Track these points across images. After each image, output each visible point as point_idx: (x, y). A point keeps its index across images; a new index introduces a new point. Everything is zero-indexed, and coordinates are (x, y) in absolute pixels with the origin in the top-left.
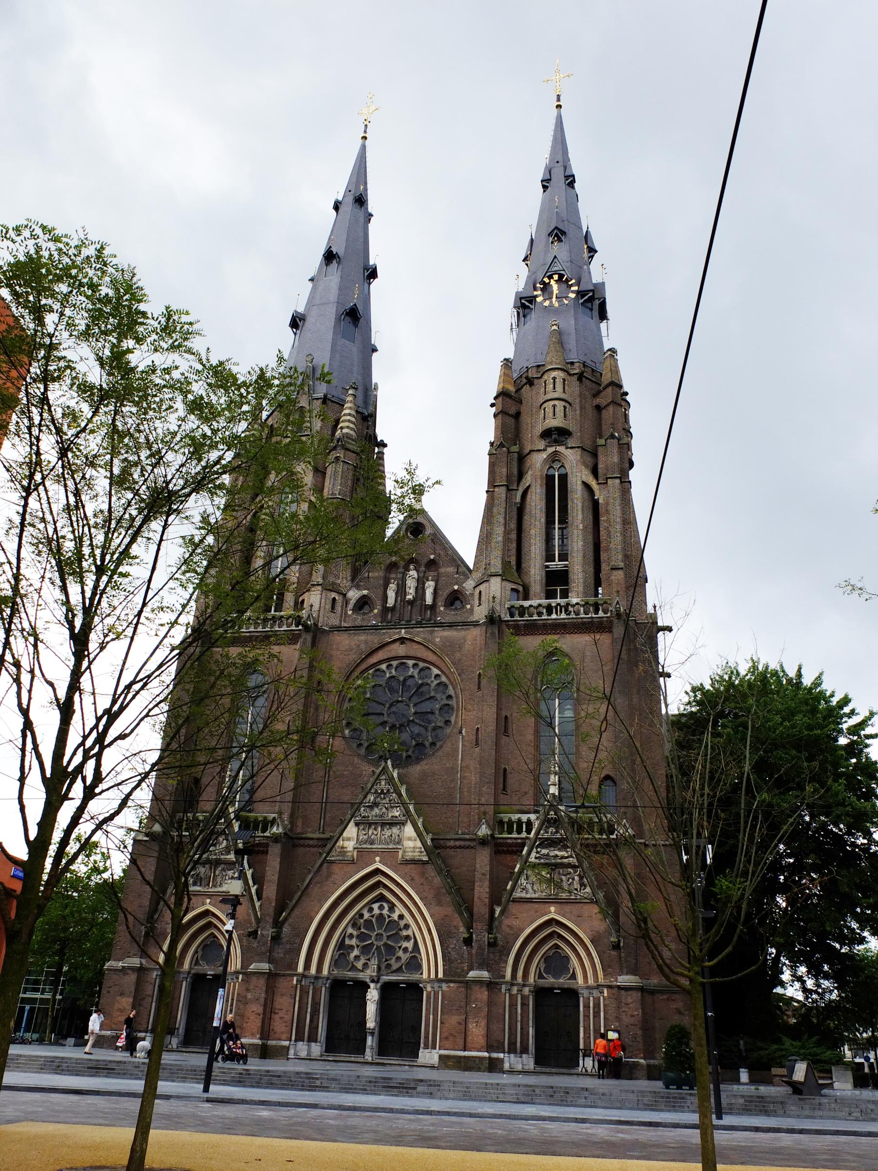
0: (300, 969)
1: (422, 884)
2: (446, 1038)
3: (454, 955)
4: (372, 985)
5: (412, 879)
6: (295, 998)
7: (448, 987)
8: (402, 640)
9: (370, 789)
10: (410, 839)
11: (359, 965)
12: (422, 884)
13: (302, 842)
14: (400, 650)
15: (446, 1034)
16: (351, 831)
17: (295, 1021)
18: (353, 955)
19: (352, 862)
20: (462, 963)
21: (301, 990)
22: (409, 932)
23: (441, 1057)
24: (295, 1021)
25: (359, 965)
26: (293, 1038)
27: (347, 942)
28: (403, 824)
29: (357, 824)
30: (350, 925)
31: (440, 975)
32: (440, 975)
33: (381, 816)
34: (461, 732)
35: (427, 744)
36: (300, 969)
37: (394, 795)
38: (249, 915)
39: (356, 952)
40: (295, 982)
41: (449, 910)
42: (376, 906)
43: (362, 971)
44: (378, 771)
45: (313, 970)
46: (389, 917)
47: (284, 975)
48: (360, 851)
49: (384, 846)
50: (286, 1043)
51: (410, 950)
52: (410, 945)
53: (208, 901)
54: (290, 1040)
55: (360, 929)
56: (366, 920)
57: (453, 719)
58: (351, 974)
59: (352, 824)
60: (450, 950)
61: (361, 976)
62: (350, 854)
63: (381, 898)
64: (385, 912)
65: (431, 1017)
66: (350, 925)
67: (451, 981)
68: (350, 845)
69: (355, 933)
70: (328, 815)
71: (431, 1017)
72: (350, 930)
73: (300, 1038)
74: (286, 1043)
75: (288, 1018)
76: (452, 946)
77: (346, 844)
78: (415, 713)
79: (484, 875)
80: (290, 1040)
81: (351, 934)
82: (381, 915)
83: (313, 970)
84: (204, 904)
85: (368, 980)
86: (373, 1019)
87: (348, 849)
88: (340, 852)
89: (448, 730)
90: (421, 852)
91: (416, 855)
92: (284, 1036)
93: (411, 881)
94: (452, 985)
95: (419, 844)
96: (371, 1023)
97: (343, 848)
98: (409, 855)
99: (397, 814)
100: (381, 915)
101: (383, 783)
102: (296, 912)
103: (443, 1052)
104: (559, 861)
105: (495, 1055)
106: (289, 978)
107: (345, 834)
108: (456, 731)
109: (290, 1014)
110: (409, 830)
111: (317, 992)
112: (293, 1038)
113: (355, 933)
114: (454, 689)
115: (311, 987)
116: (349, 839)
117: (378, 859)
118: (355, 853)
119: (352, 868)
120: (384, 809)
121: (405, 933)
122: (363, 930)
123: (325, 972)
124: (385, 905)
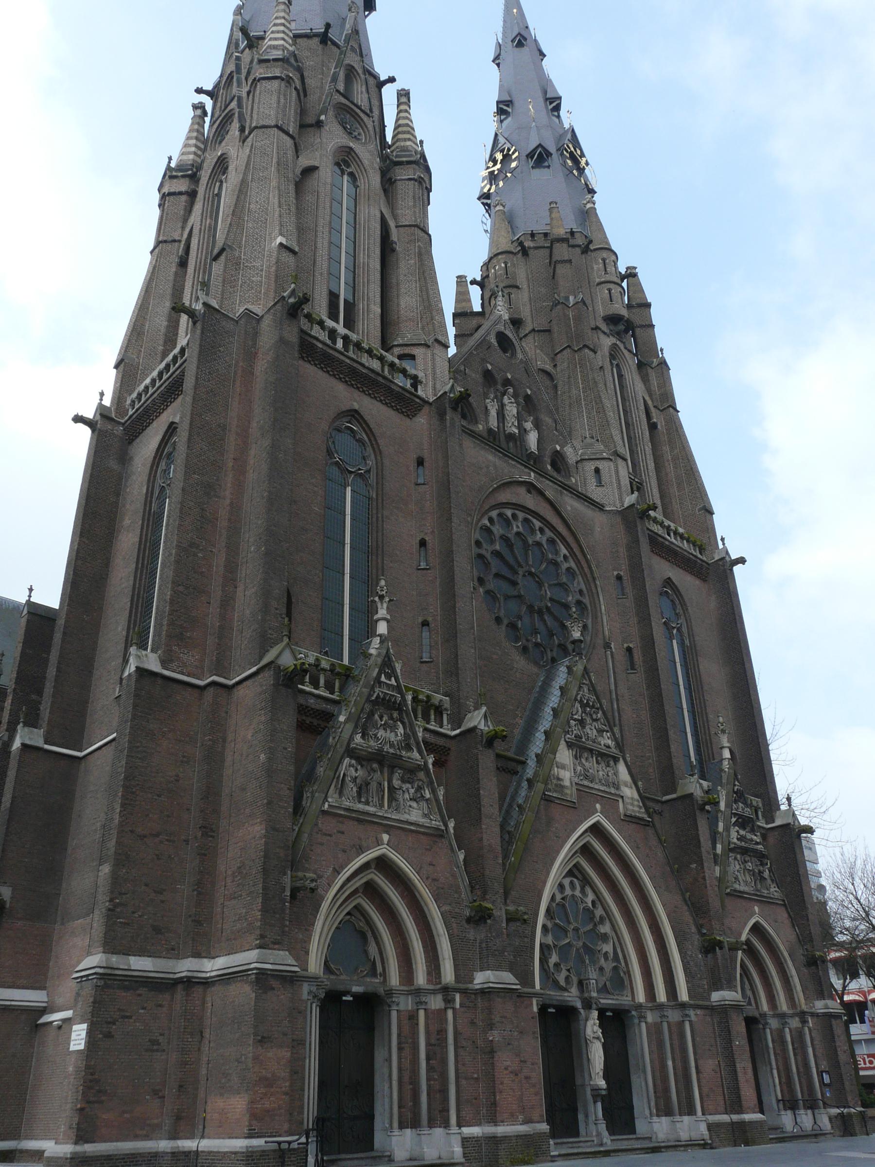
5: (638, 847)
8: (530, 487)
14: (530, 501)
22: (605, 928)
23: (710, 1127)
28: (616, 760)
31: (684, 996)
32: (684, 996)
34: (607, 646)
38: (454, 876)
48: (581, 790)
49: (602, 788)
52: (608, 948)
53: (386, 837)
56: (557, 904)
65: (670, 1063)
71: (670, 1063)
78: (551, 599)
82: (573, 896)
84: (379, 842)
100: (573, 896)
103: (712, 1118)
104: (751, 846)
105: (735, 1117)
108: (600, 642)
114: (587, 582)
116: (563, 767)
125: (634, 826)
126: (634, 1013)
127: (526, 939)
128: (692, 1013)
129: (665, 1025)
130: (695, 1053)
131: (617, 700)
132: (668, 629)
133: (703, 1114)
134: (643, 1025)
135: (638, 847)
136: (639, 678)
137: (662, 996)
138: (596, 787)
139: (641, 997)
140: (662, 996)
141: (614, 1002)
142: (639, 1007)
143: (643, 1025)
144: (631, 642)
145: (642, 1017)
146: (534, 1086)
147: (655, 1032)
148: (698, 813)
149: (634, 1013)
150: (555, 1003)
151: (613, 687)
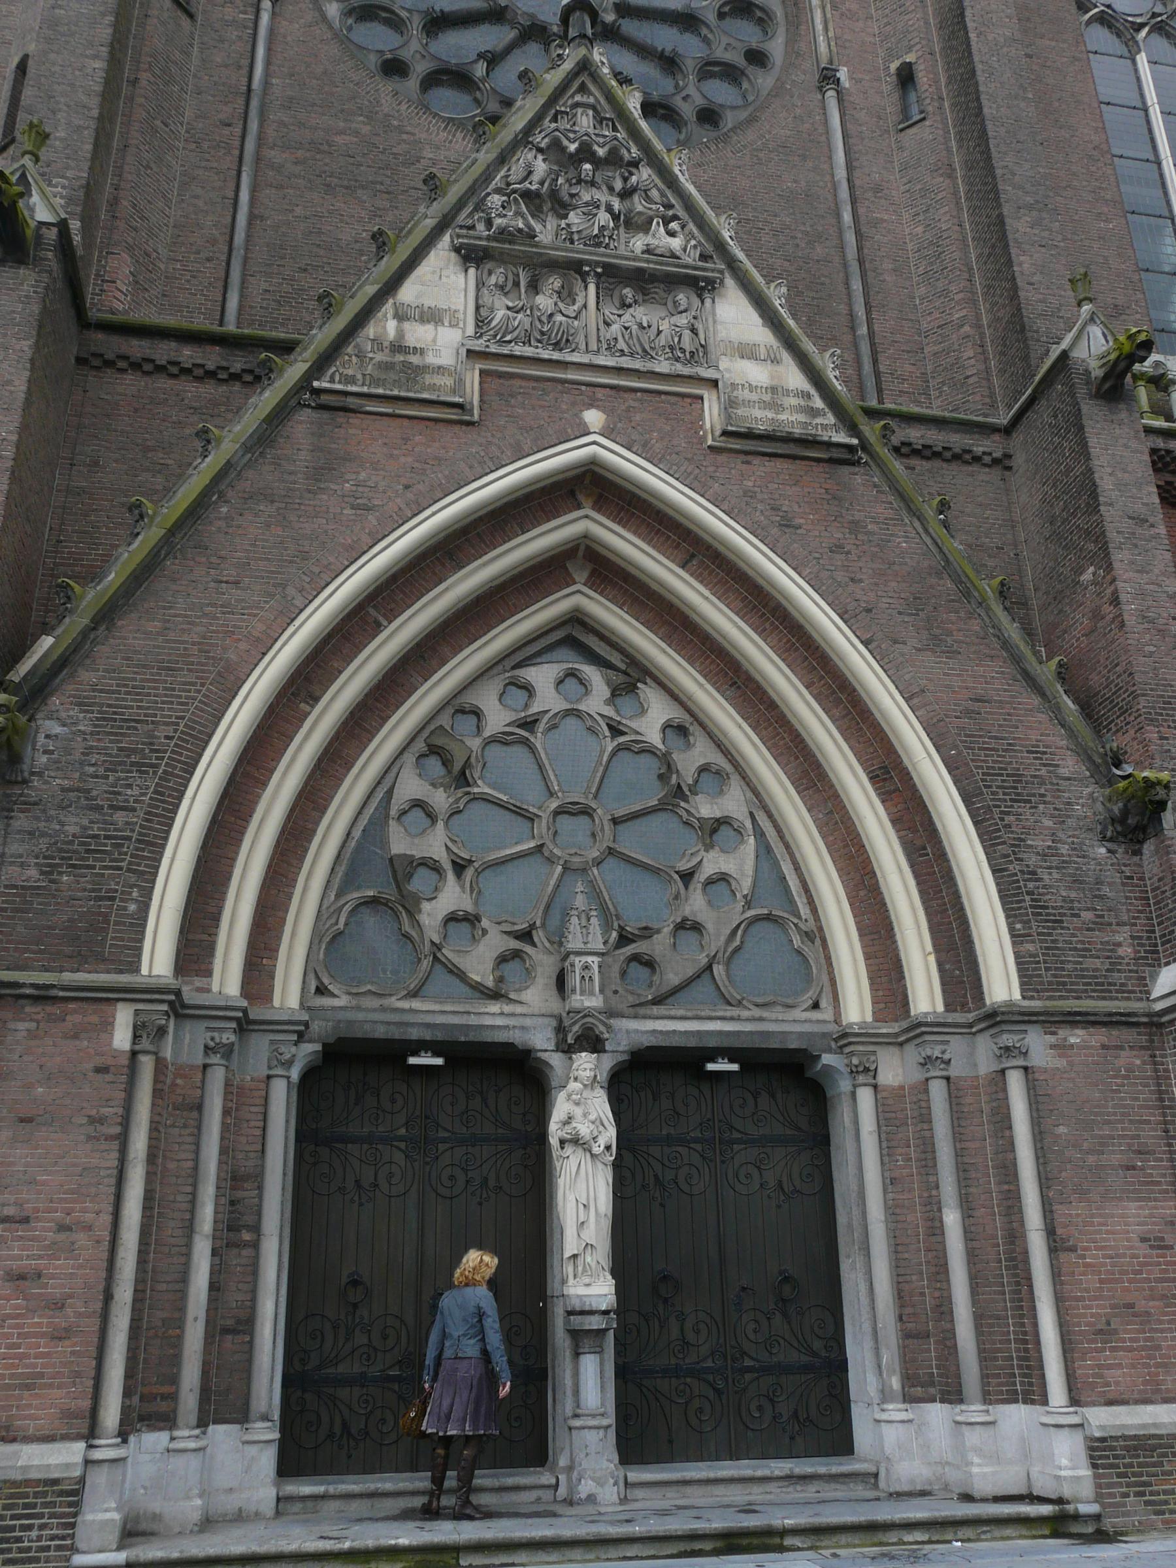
0: (158, 957)
1: (837, 548)
2: (1105, 1333)
3: (1056, 888)
4: (585, 1063)
5: (787, 524)
6: (123, 1140)
7: (1061, 1048)
9: (529, 130)
10: (747, 352)
11: (479, 963)
12: (837, 548)
13: (137, 348)
15: (1091, 1312)
16: (442, 283)
17: (124, 1293)
18: (432, 914)
19: (455, 416)
20: (1100, 924)
21: (157, 1093)
22: (732, 803)
23: (1100, 1450)
24: (124, 1293)
25: (479, 963)
26: (111, 1415)
27: (400, 843)
28: (704, 287)
29: (470, 256)
30: (409, 758)
32: (1001, 983)
33: (596, 241)
34: (828, 77)
35: (687, 111)
36: (158, 957)
37: (645, 174)
39: (453, 896)
40: (122, 1038)
41: (993, 677)
42: (543, 676)
43: (495, 995)
44: (553, 78)
45: (227, 977)
46: (616, 730)
47: (43, 996)
50: (62, 1457)
51: (746, 885)
54: (91, 1434)
55: (462, 779)
57: (776, 48)
58: (435, 1012)
59: (440, 257)
60: (1032, 860)
61: (494, 1020)
62: (447, 381)
63: (575, 636)
64: (597, 702)
65: (952, 1219)
66: (409, 758)
67: (1073, 1019)
68: (443, 345)
69: (440, 800)
70: (258, 285)
71: (952, 1219)
72: (410, 786)
73: (149, 1410)
74: (62, 1457)
75: (68, 1274)
76: (1039, 842)
77: (418, 334)
79: (1141, 521)
80: (91, 1434)
81: (418, 804)
83: (227, 977)
85: (541, 1040)
86: (600, 1256)
87: (431, 359)
88: (387, 367)
89: (764, 81)
90: (813, 412)
91: (791, 420)
92: (40, 1410)
93: (779, 532)
94: (1075, 1037)
95: (795, 379)
96: (588, 1282)
97: (398, 347)
98: (760, 418)
99: (676, 243)
101: (585, 121)
102: (135, 634)
106: (76, 1017)
107: (408, 293)
109: (89, 1248)
110: (733, 316)
111: (244, 1104)
112: (111, 1415)
113: (440, 800)
115: (217, 1077)
116: (431, 316)
117: (593, 417)
118: (473, 380)
119: (451, 442)
120: (603, 217)
121: (705, 808)
122: (482, 788)
123: (288, 992)
124: (591, 673)
125: (771, 465)
126: (827, 1059)
127: (120, 817)
128: (1038, 1046)
129: (938, 1092)
130: (1044, 1182)
131: (854, 202)
132: (1119, 35)
133: (1074, 1401)
134: (865, 1097)
135: (787, 524)
136: (934, 135)
137: (925, 994)
138: (576, 358)
139: (856, 1005)
140: (925, 994)
141: (748, 1027)
142: (844, 1039)
143: (865, 1097)
144: (910, 49)
145: (866, 1071)
146: (58, 1306)
147: (902, 1117)
148: (1092, 413)
149: (827, 1059)
150: (439, 1036)
151: (841, 173)
